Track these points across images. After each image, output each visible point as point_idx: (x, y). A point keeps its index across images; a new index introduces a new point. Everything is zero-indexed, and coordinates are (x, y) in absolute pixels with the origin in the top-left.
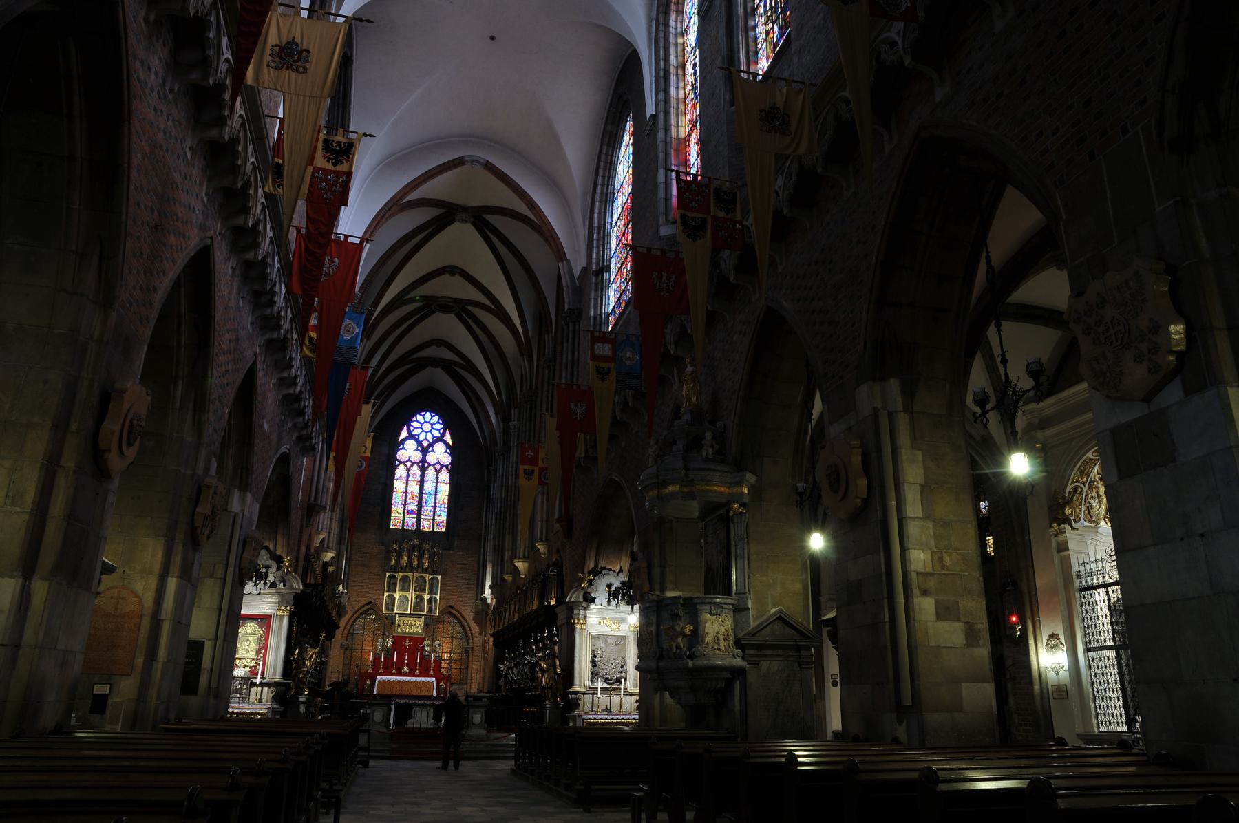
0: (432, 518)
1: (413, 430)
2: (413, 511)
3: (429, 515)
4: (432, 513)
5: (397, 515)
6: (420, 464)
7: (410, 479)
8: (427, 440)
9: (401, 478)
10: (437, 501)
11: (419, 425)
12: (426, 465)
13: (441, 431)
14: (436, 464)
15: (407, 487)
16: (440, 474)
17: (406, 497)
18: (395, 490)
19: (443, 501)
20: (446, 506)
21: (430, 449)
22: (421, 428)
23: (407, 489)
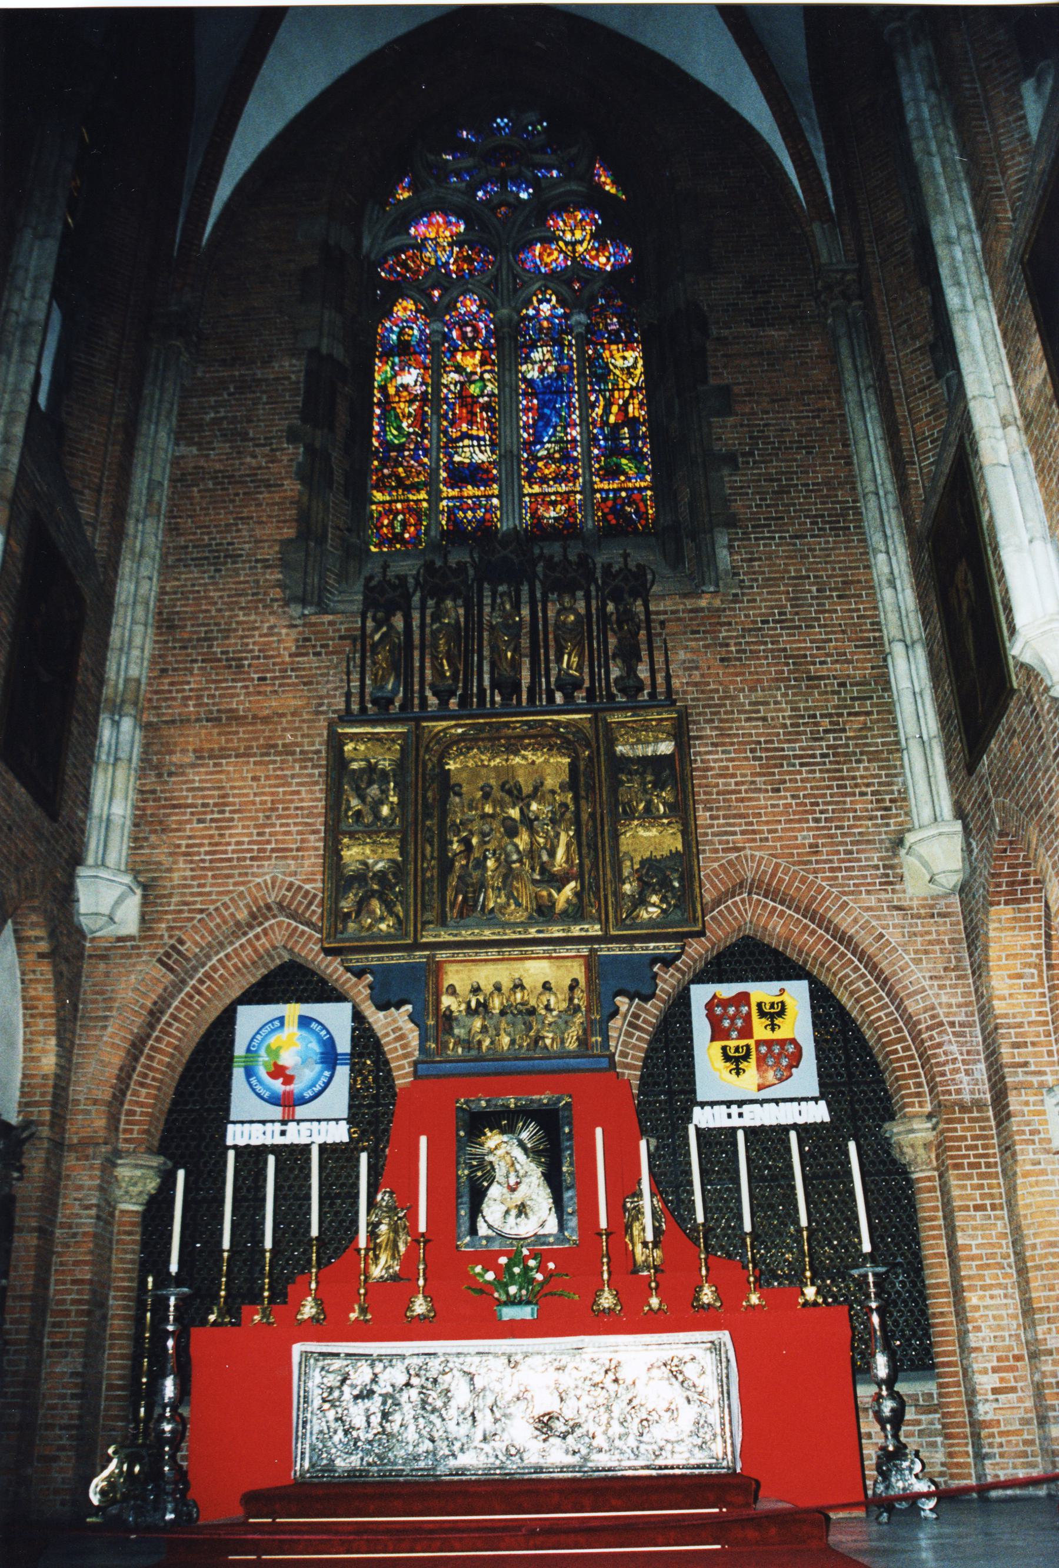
9: (404, 349)
19: (624, 408)
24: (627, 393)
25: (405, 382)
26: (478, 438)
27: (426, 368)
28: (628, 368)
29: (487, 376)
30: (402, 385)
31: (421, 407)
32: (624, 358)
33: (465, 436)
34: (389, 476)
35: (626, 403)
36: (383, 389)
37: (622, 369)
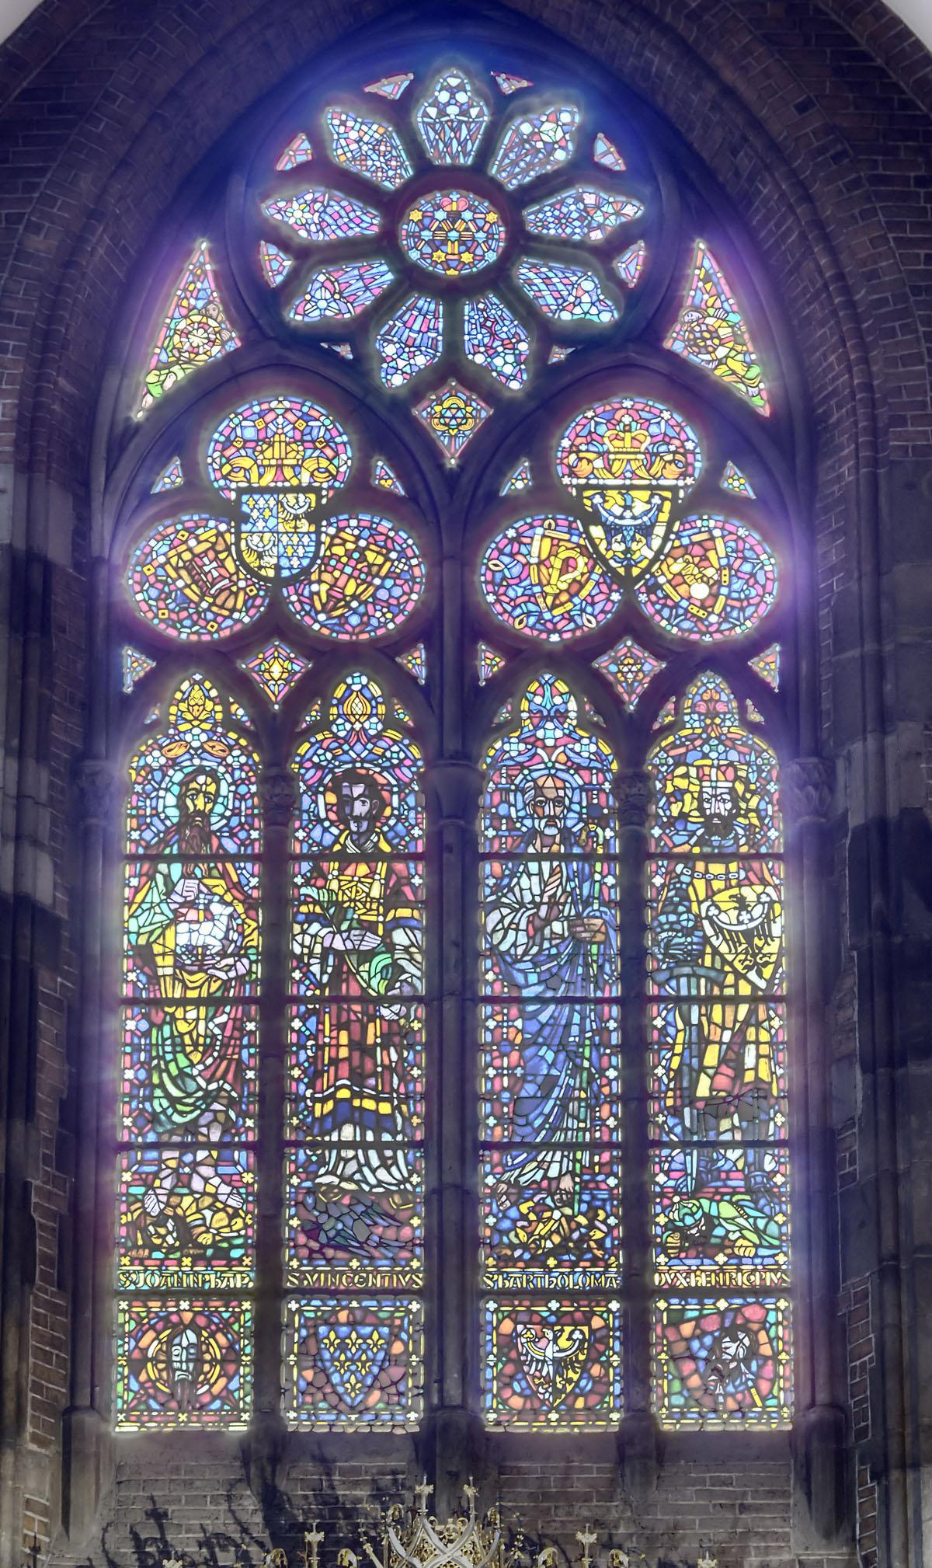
0: (612, 1279)
1: (295, 280)
2: (369, 1207)
3: (574, 1249)
4: (608, 1225)
5: (186, 1272)
6: (416, 662)
7: (300, 839)
8: (477, 383)
10: (662, 1069)
11: (369, 223)
12: (489, 663)
13: (631, 265)
14: (605, 639)
15: (277, 930)
16: (657, 757)
17: (273, 1050)
18: (129, 979)
19: (732, 1058)
20: (778, 1124)
21: (518, 481)
22: (386, 245)
23: (276, 957)
24: (743, 1009)
25: (197, 940)
26: (380, 1123)
27: (250, 905)
28: (749, 935)
29: (400, 937)
30: (190, 949)
31: (238, 1025)
32: (742, 904)
33: (345, 1113)
34: (161, 1220)
35: (740, 1041)
36: (144, 956)
37: (732, 939)
